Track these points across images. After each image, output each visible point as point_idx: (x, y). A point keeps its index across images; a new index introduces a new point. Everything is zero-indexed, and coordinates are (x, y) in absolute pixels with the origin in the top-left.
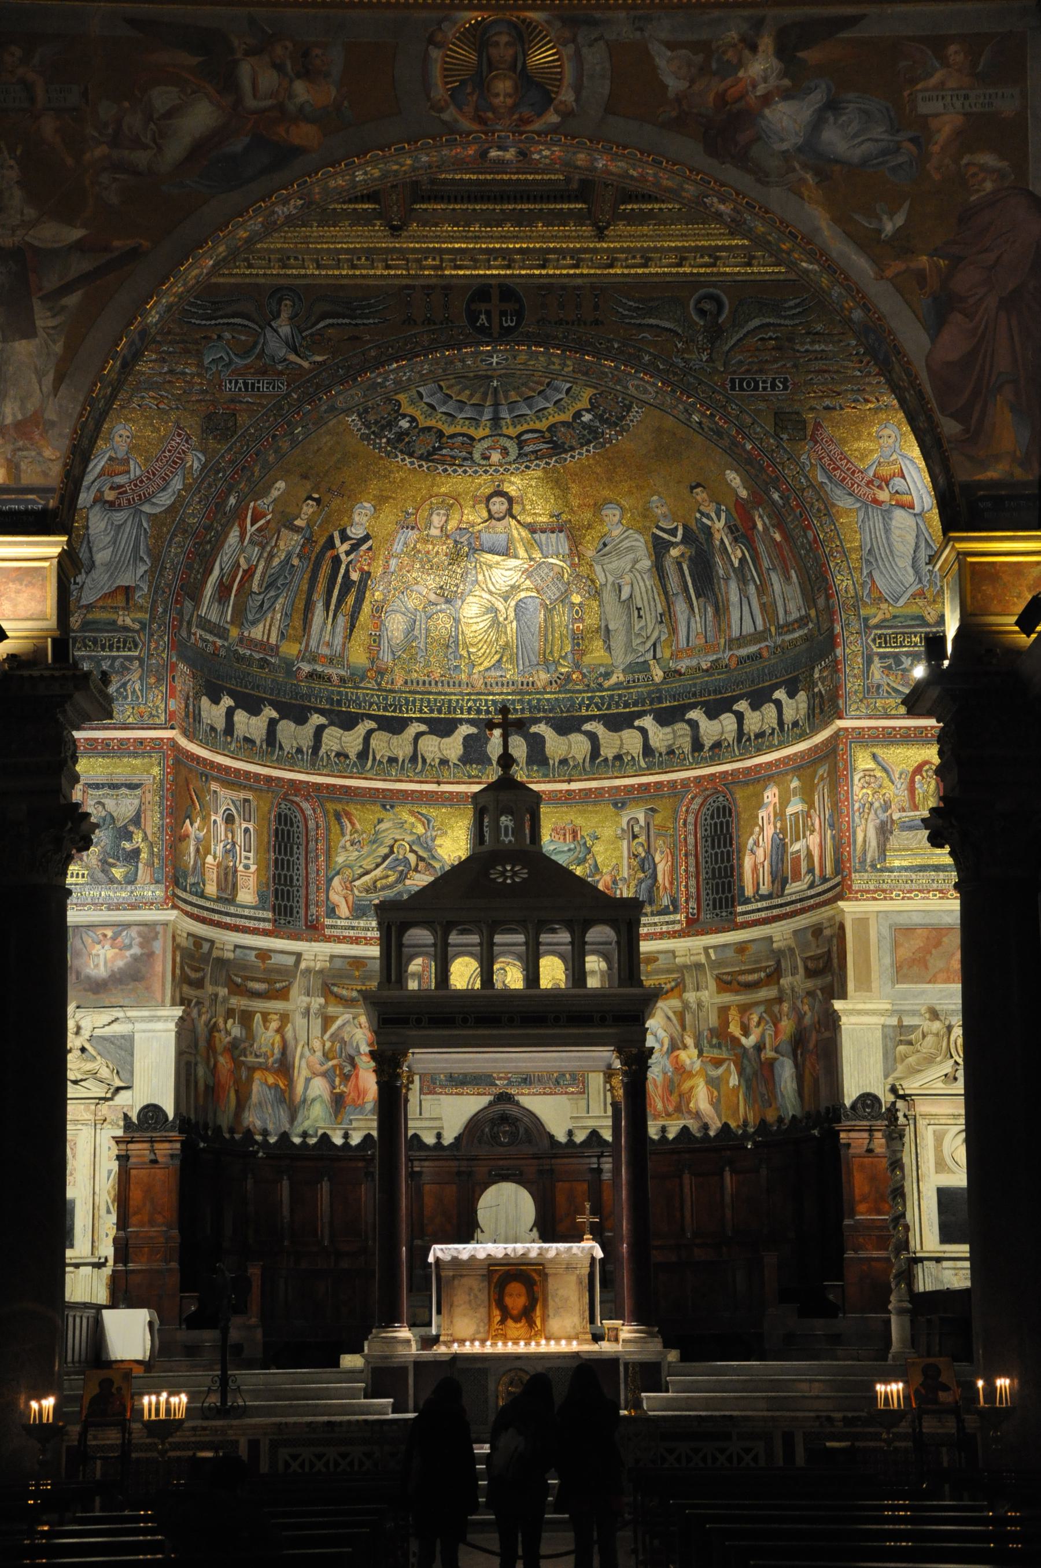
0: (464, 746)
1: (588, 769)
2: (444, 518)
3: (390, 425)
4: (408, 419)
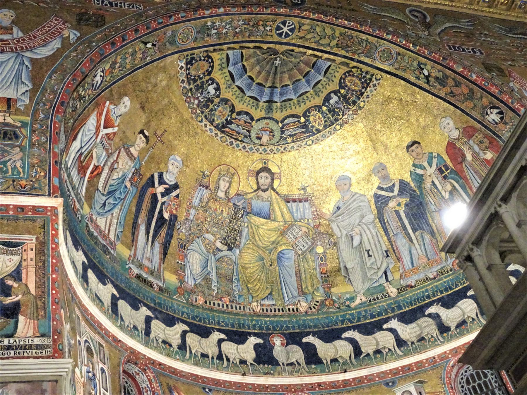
0: (255, 351)
1: (355, 363)
2: (228, 184)
3: (201, 88)
4: (215, 85)
